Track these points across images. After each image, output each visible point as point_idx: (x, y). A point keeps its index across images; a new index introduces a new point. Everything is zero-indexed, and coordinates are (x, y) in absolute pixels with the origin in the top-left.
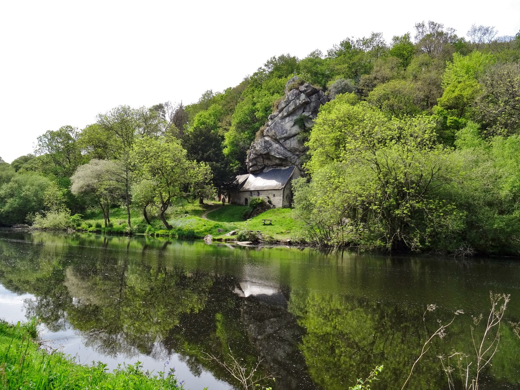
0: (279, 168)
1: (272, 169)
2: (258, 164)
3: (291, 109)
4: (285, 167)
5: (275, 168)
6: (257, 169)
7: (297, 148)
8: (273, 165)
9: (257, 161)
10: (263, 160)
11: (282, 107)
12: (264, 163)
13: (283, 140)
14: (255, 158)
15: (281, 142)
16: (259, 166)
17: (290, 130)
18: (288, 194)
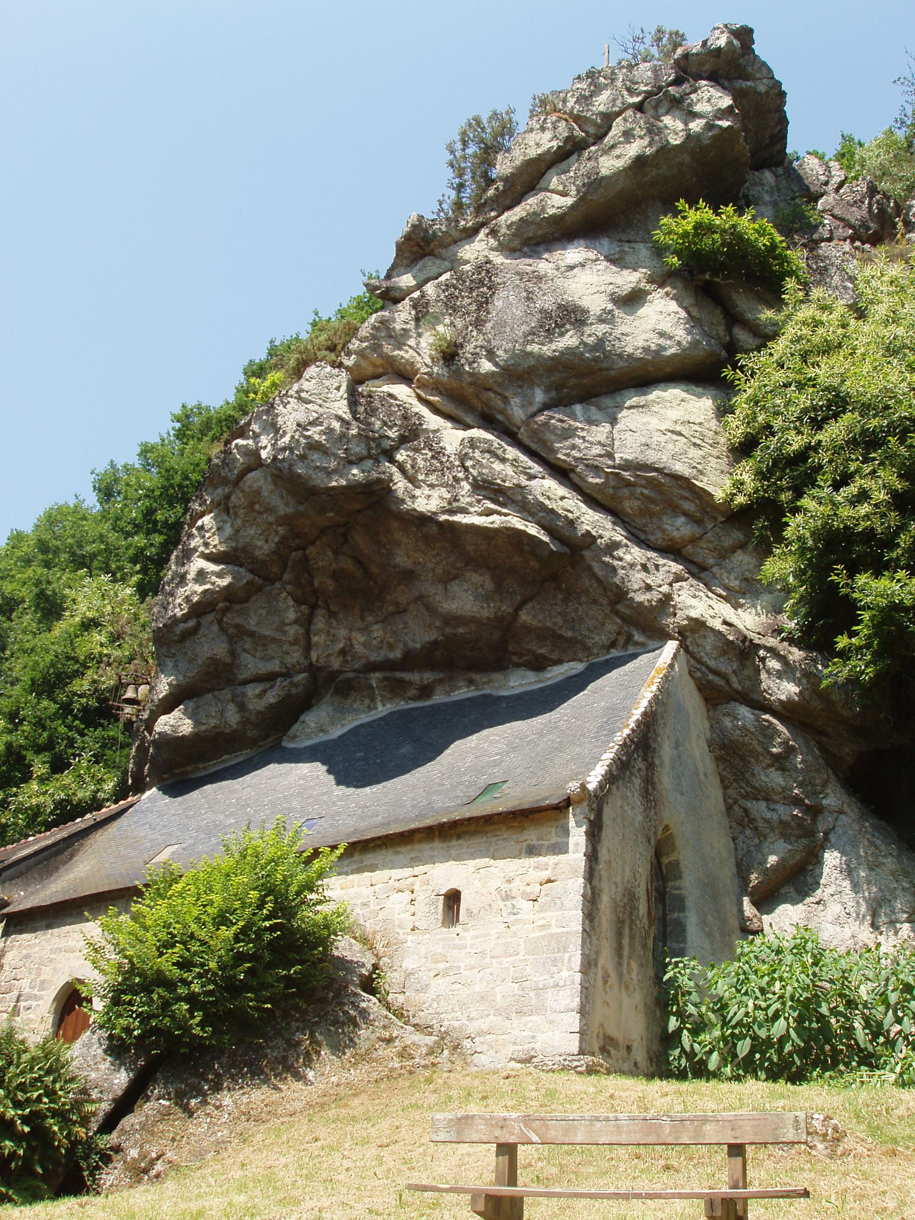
0: (463, 693)
1: (382, 709)
2: (251, 664)
3: (620, 164)
4: (539, 665)
5: (426, 691)
6: (233, 717)
7: (680, 468)
8: (409, 661)
9: (243, 632)
10: (306, 623)
11: (533, 153)
12: (308, 648)
13: (539, 396)
14: (228, 594)
15: (517, 411)
16: (252, 690)
17: (606, 318)
18: (631, 897)
